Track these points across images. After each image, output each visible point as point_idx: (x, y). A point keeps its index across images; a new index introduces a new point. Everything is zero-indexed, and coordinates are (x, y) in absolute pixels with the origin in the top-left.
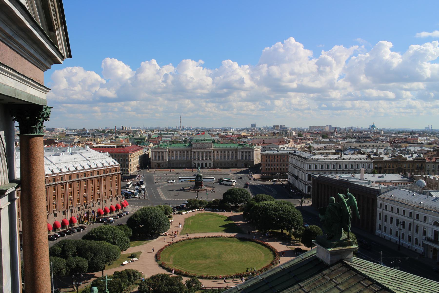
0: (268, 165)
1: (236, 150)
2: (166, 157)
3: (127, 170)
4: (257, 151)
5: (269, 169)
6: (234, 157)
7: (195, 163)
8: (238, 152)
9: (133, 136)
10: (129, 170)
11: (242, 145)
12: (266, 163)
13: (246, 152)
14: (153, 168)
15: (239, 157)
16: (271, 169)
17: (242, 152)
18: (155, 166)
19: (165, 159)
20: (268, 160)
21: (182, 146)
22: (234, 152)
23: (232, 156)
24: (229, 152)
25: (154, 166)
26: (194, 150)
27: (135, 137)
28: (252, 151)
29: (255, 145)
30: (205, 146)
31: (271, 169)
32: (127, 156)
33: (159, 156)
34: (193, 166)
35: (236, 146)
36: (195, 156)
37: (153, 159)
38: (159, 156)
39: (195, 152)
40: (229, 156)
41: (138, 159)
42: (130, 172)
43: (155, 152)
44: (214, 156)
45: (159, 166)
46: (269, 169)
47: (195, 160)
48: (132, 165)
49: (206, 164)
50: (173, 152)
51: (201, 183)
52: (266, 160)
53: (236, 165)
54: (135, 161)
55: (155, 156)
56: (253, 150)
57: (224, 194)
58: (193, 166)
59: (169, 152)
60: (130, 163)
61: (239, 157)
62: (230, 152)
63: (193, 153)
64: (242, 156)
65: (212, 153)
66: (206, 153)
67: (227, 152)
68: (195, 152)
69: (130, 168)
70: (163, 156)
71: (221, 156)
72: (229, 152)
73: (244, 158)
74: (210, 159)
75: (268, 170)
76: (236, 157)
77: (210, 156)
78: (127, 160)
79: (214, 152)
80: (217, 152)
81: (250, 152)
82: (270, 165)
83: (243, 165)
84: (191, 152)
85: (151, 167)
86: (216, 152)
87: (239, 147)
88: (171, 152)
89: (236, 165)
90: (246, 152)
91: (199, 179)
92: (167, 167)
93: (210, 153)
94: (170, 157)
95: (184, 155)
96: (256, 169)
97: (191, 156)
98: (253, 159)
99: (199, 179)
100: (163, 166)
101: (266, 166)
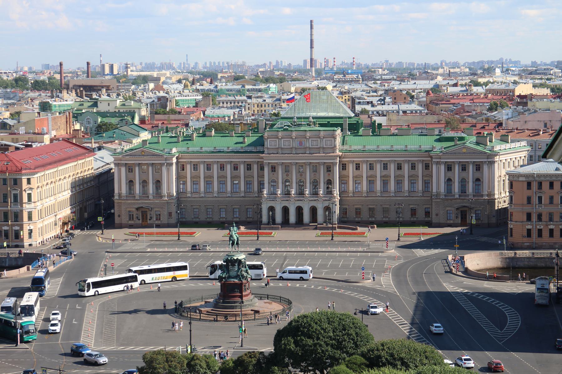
0: (534, 218)
1: (427, 160)
2: (171, 187)
3: (17, 235)
4: (510, 158)
5: (540, 231)
6: (420, 186)
7: (272, 209)
8: (434, 167)
9: (95, 105)
10: (25, 234)
11: (451, 139)
12: (528, 209)
13: (464, 168)
14: (121, 227)
15: (438, 185)
16: (546, 233)
17: (449, 168)
18: (131, 217)
19: (165, 191)
20: (535, 200)
21: (229, 143)
22: (420, 167)
23: (412, 182)
24: (399, 167)
25: (125, 219)
26: (268, 159)
27: (102, 107)
28: (484, 162)
29: (504, 139)
30: (308, 144)
31: (546, 233)
32: (17, 182)
33: (144, 183)
34: (265, 219)
35: (427, 143)
36: (273, 183)
37: (124, 191)
38: (144, 183)
39: (273, 169)
40: (399, 182)
41: (67, 194)
42: (26, 243)
43: (130, 169)
44: (343, 181)
45: (143, 219)
46: (540, 231)
47: (272, 198)
48: (35, 216)
49: (314, 210)
50: (195, 167)
51: (240, 287)
52: (529, 199)
53: (427, 214)
54: (49, 202)
55: (131, 183)
56: (490, 159)
57: (279, 331)
58: (265, 219)
59: (181, 167)
60: (27, 207)
61: (438, 185)
62: (406, 167)
63: (266, 170)
64: (449, 181)
65: (337, 169)
66: (315, 169)
67: (392, 168)
68: (273, 169)
69: (26, 228)
70: (158, 184)
71: (371, 182)
72: (399, 167)
73: (456, 188)
74: (329, 192)
75: (534, 234)
76: (427, 184)
77: (329, 182)
78: (15, 196)
79: (344, 167)
80: (358, 167)
81: (478, 167)
82: (545, 218)
83: (453, 216)
84: (262, 169)
85: (117, 220)
86: (351, 168)
87: (439, 146)
88: (188, 168)
89: (427, 214)
90: (464, 168)
91: (233, 273)
92: (173, 221)
93: (329, 169)
94: (185, 183)
95: (222, 181)
96: (487, 229)
97: (261, 185)
98: (491, 194)
99: (233, 273)
100: (158, 217)
101: (529, 217)
